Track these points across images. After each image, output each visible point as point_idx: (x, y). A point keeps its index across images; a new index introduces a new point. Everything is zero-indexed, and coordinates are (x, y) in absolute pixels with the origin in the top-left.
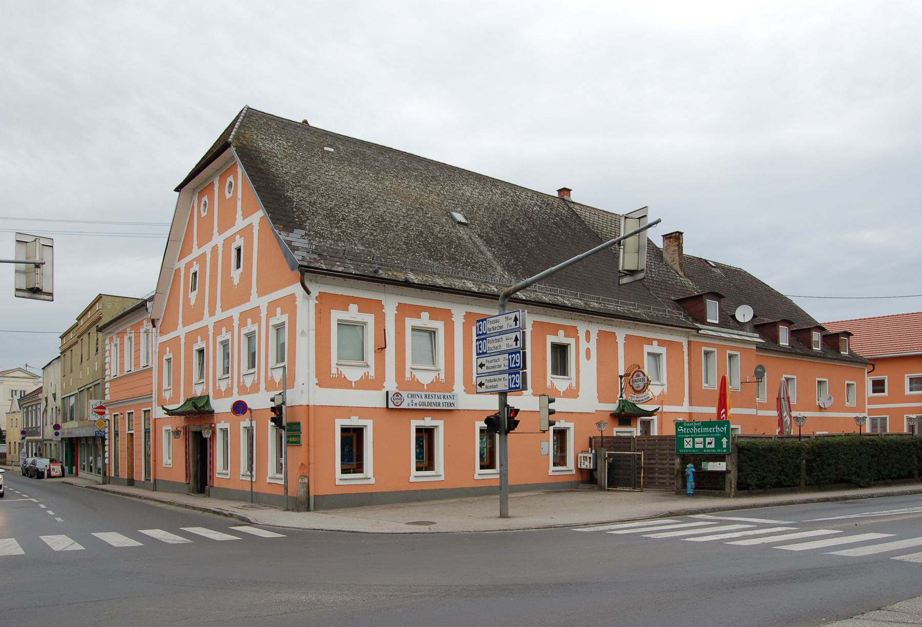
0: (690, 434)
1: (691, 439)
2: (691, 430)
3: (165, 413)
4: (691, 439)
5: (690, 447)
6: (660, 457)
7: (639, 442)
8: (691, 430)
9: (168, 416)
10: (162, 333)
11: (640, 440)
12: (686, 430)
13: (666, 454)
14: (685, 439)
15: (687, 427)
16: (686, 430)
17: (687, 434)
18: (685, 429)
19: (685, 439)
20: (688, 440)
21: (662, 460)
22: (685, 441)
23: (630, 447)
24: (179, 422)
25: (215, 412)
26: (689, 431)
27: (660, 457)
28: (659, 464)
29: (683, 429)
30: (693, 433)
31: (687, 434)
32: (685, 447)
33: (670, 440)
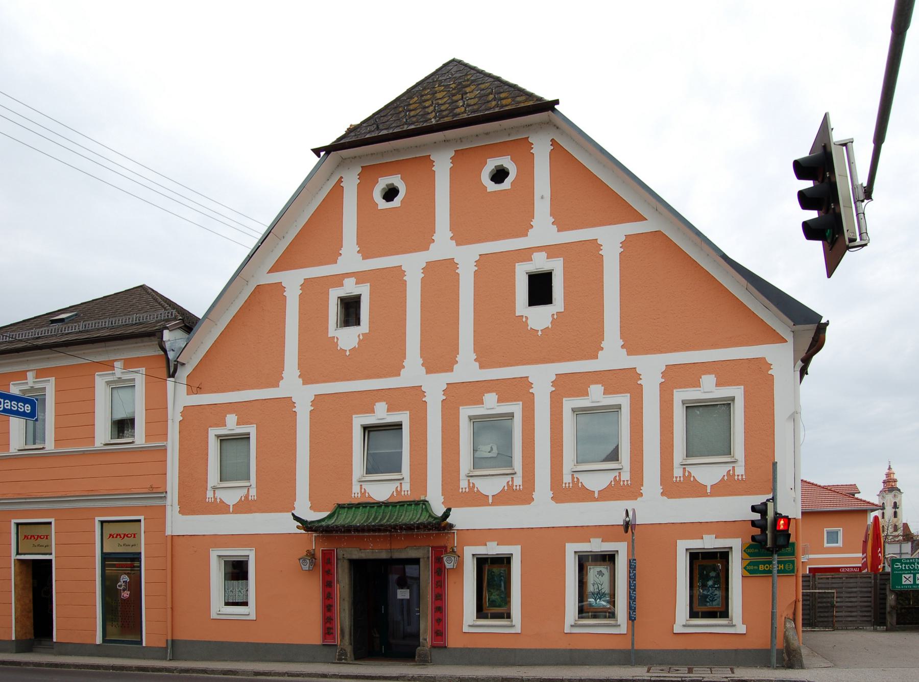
0: (910, 570)
1: (912, 575)
2: (912, 567)
3: (298, 527)
4: (912, 575)
5: (910, 583)
6: (848, 595)
7: (821, 581)
8: (912, 567)
9: (303, 531)
10: (195, 388)
11: (821, 578)
12: (905, 567)
13: (856, 592)
14: (903, 575)
15: (906, 563)
16: (905, 567)
17: (906, 570)
18: (903, 565)
19: (903, 575)
20: (907, 576)
21: (850, 597)
22: (903, 578)
23: (809, 586)
24: (311, 542)
25: (454, 528)
26: (908, 567)
27: (848, 595)
28: (847, 602)
29: (901, 565)
30: (914, 569)
31: (906, 570)
32: (903, 583)
33: (860, 577)
